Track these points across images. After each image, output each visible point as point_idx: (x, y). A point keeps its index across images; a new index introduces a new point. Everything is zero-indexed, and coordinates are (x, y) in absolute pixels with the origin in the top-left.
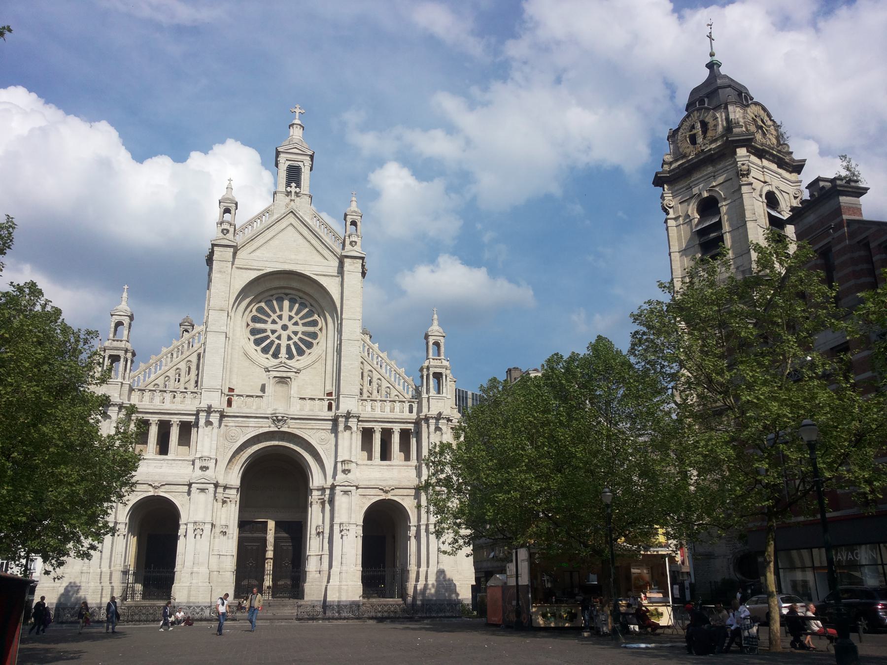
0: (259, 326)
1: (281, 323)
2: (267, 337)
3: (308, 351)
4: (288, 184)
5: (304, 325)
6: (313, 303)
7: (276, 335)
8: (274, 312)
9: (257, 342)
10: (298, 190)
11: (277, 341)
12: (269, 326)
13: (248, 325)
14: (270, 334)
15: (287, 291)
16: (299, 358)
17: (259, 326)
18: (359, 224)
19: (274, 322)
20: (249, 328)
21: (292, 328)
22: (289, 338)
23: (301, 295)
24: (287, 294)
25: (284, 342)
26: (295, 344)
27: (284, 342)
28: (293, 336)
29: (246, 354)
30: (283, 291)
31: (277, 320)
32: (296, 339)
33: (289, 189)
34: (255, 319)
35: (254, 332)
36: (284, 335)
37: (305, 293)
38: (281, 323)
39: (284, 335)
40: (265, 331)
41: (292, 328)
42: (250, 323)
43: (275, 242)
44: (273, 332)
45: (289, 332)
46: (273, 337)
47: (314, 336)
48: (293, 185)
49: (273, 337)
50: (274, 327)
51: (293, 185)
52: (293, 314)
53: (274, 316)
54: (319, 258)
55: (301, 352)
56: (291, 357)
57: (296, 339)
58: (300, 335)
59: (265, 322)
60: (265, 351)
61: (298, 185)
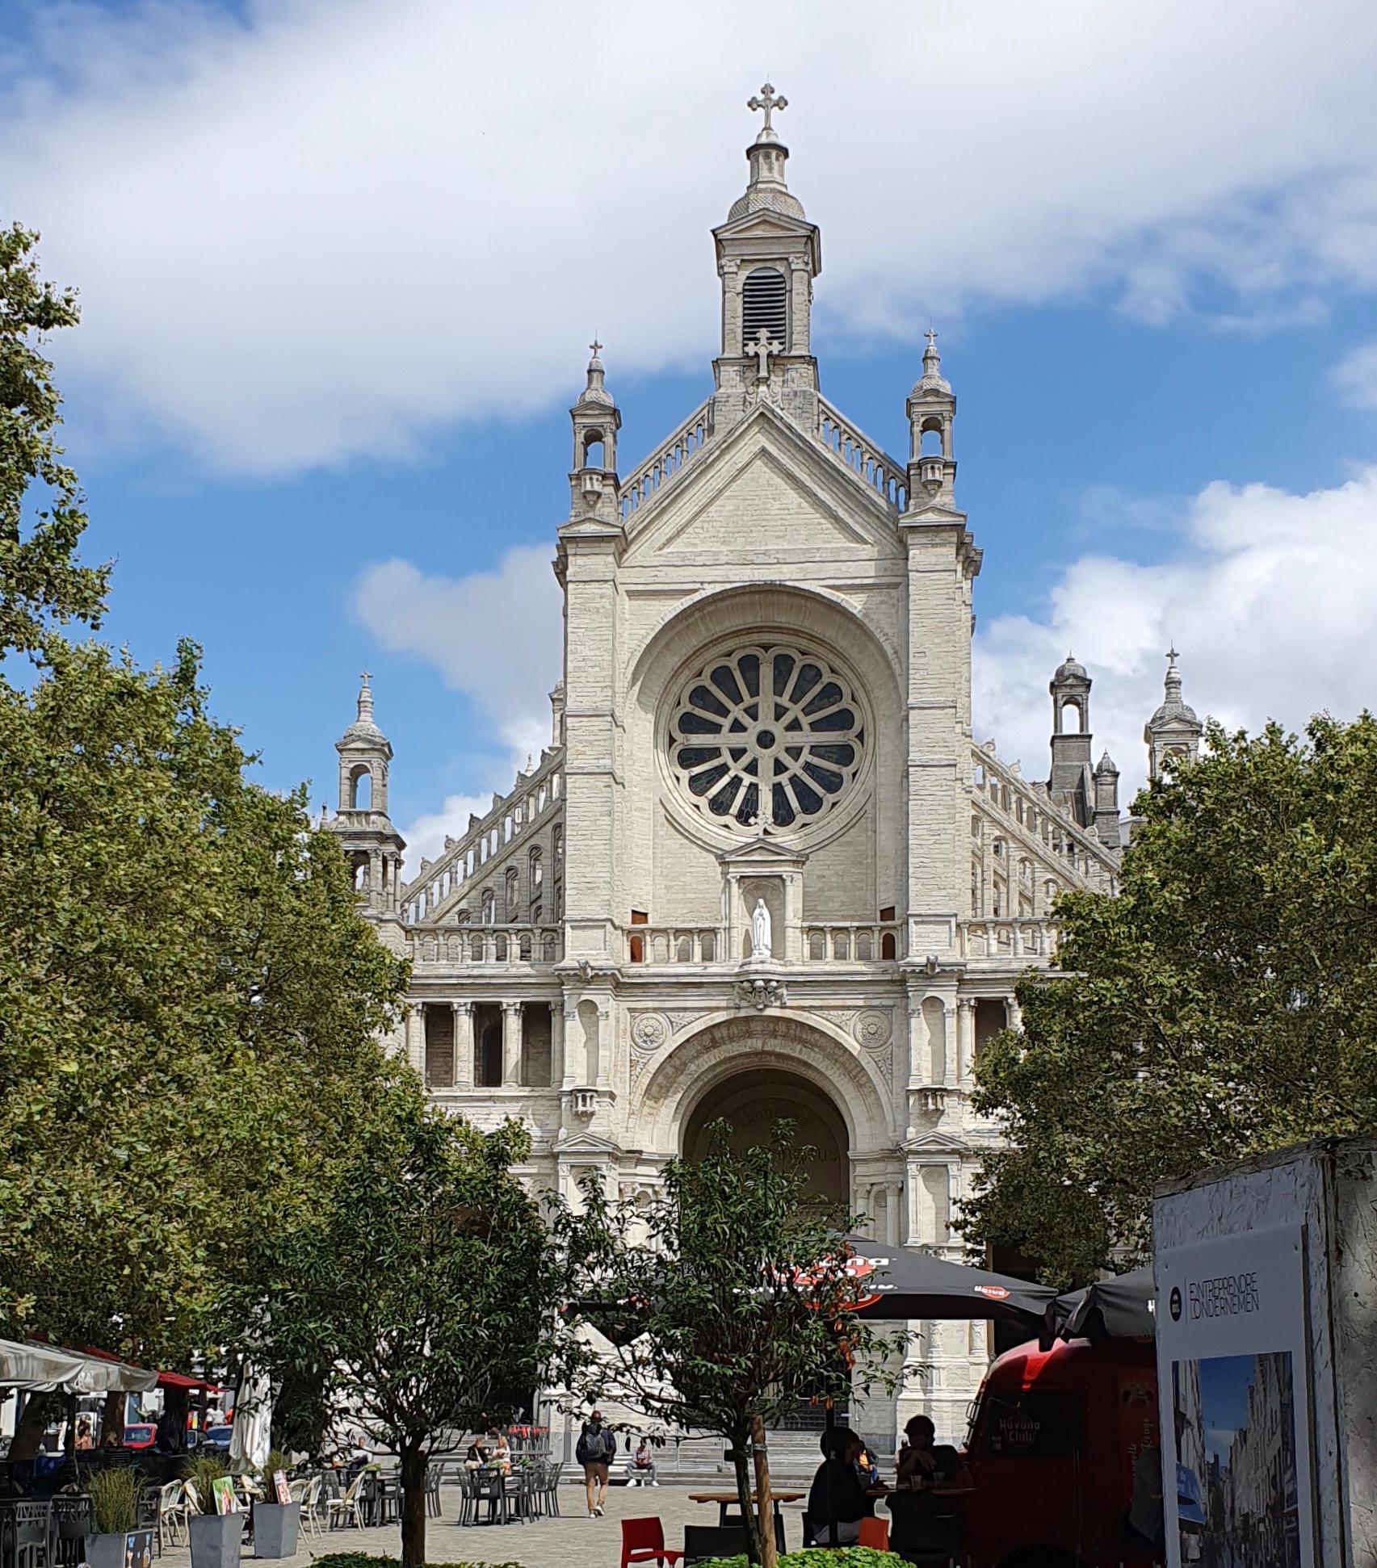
0: (699, 740)
1: (754, 728)
2: (723, 769)
3: (829, 799)
4: (750, 336)
5: (815, 727)
6: (837, 663)
7: (745, 760)
8: (737, 699)
9: (698, 785)
10: (776, 347)
12: (725, 740)
13: (672, 740)
14: (730, 762)
15: (767, 638)
16: (808, 818)
17: (699, 740)
18: (947, 426)
19: (737, 727)
20: (677, 749)
21: (784, 739)
22: (780, 768)
23: (804, 644)
24: (766, 647)
26: (794, 780)
28: (787, 760)
29: (671, 820)
30: (756, 638)
31: (746, 720)
32: (795, 768)
33: (751, 349)
35: (687, 758)
37: (811, 638)
38: (754, 728)
40: (715, 752)
41: (784, 739)
42: (678, 735)
43: (724, 506)
47: (845, 755)
48: (763, 333)
49: (735, 769)
53: (737, 712)
54: (841, 541)
55: (811, 803)
56: (783, 816)
57: (795, 768)
58: (805, 756)
59: (716, 729)
60: (719, 806)
61: (779, 333)
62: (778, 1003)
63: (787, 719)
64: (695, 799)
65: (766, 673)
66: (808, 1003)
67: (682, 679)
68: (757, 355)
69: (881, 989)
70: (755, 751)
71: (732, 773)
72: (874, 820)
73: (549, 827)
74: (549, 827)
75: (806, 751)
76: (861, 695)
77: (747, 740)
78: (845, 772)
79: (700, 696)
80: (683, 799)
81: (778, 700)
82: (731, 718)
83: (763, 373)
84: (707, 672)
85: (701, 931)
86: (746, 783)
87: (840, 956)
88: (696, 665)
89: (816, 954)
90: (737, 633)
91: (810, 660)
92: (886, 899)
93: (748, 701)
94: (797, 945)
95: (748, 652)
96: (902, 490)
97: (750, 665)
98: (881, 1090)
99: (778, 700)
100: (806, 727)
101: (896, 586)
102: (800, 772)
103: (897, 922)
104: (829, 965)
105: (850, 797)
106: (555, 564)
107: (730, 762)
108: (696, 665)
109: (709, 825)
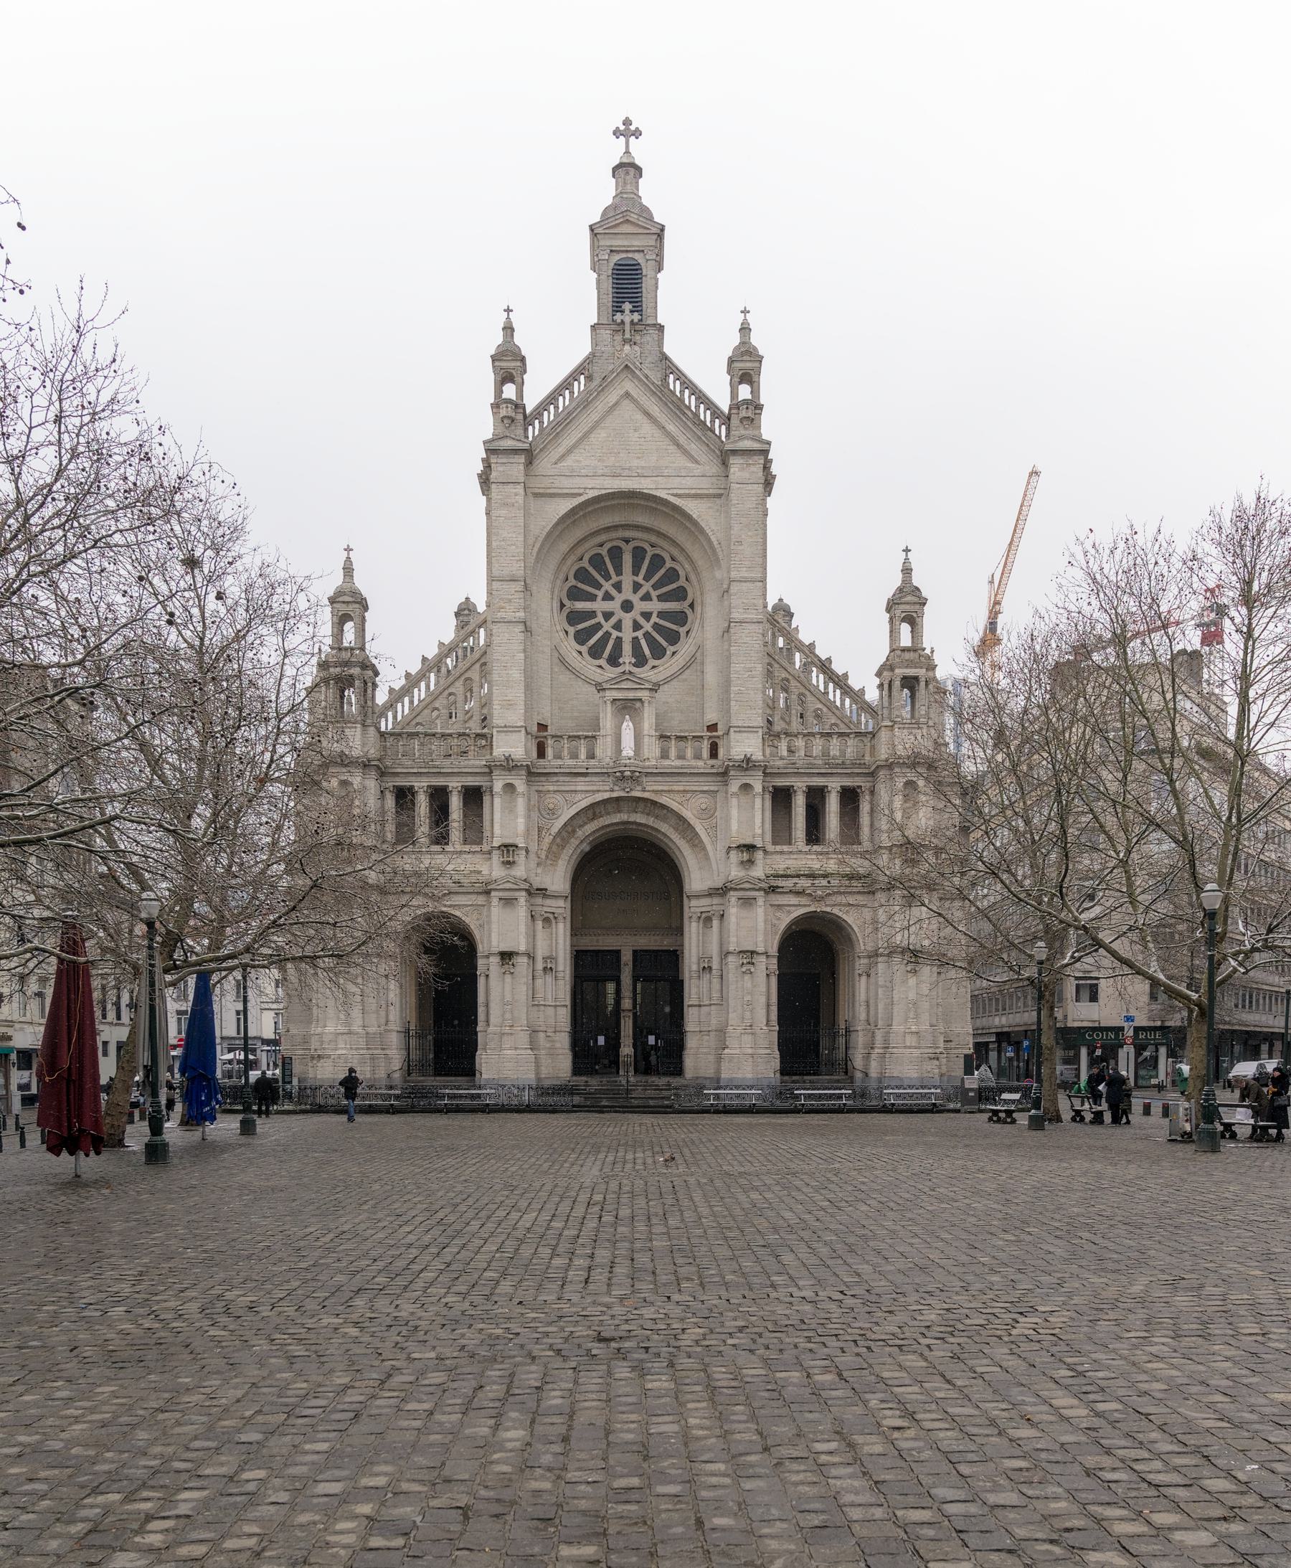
0: (581, 605)
1: (619, 598)
4: (617, 309)
5: (661, 598)
6: (676, 553)
7: (613, 620)
9: (581, 638)
10: (636, 317)
11: (615, 634)
12: (599, 606)
13: (562, 606)
14: (603, 621)
15: (628, 534)
16: (656, 662)
17: (581, 605)
19: (608, 597)
21: (640, 606)
22: (637, 627)
23: (653, 539)
24: (627, 541)
25: (627, 635)
26: (647, 635)
27: (627, 635)
28: (642, 621)
29: (562, 661)
30: (621, 534)
31: (613, 592)
32: (648, 627)
34: (574, 594)
35: (574, 617)
36: (627, 619)
39: (627, 619)
40: (592, 614)
41: (640, 606)
42: (566, 601)
44: (608, 616)
45: (635, 614)
46: (607, 626)
47: (681, 618)
48: (627, 307)
50: (608, 606)
51: (627, 307)
52: (640, 579)
53: (607, 586)
55: (659, 652)
56: (640, 661)
57: (648, 627)
58: (654, 619)
59: (592, 598)
60: (595, 653)
61: (637, 308)
62: (639, 788)
63: (642, 592)
64: (579, 647)
65: (627, 560)
66: (660, 788)
67: (569, 562)
68: (623, 322)
69: (710, 779)
70: (620, 614)
71: (604, 630)
72: (703, 664)
73: (478, 665)
74: (478, 665)
75: (654, 615)
76: (693, 577)
77: (614, 606)
78: (682, 630)
79: (581, 575)
80: (570, 647)
81: (636, 578)
82: (603, 590)
83: (627, 336)
84: (586, 558)
85: (586, 737)
86: (614, 636)
87: (681, 757)
88: (579, 552)
89: (665, 755)
90: (607, 529)
91: (658, 551)
92: (711, 717)
93: (615, 578)
94: (652, 749)
95: (615, 543)
96: (723, 427)
97: (616, 553)
98: (709, 847)
99: (636, 578)
100: (655, 598)
101: (720, 496)
102: (650, 630)
103: (720, 733)
104: (673, 763)
105: (685, 648)
106: (480, 476)
107: (603, 621)
108: (579, 552)
109: (589, 667)
